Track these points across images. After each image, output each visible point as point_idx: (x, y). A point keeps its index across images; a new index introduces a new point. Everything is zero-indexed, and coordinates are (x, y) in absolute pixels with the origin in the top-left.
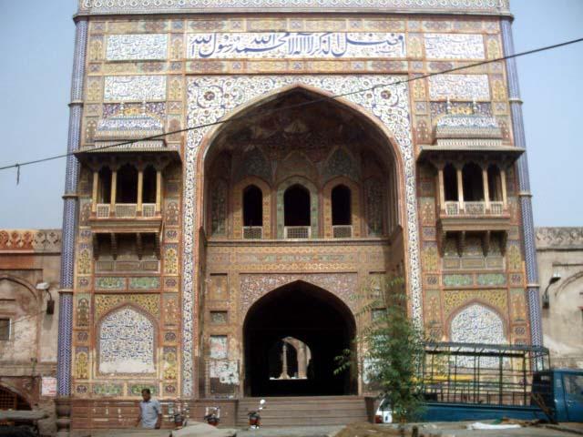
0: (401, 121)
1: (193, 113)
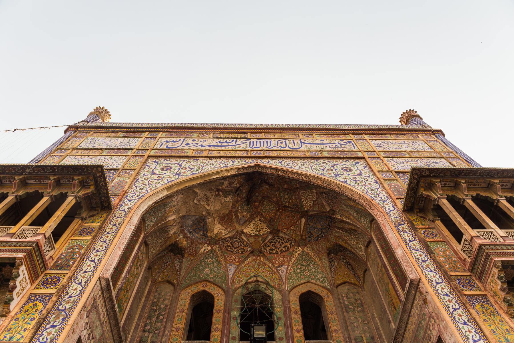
0: (370, 184)
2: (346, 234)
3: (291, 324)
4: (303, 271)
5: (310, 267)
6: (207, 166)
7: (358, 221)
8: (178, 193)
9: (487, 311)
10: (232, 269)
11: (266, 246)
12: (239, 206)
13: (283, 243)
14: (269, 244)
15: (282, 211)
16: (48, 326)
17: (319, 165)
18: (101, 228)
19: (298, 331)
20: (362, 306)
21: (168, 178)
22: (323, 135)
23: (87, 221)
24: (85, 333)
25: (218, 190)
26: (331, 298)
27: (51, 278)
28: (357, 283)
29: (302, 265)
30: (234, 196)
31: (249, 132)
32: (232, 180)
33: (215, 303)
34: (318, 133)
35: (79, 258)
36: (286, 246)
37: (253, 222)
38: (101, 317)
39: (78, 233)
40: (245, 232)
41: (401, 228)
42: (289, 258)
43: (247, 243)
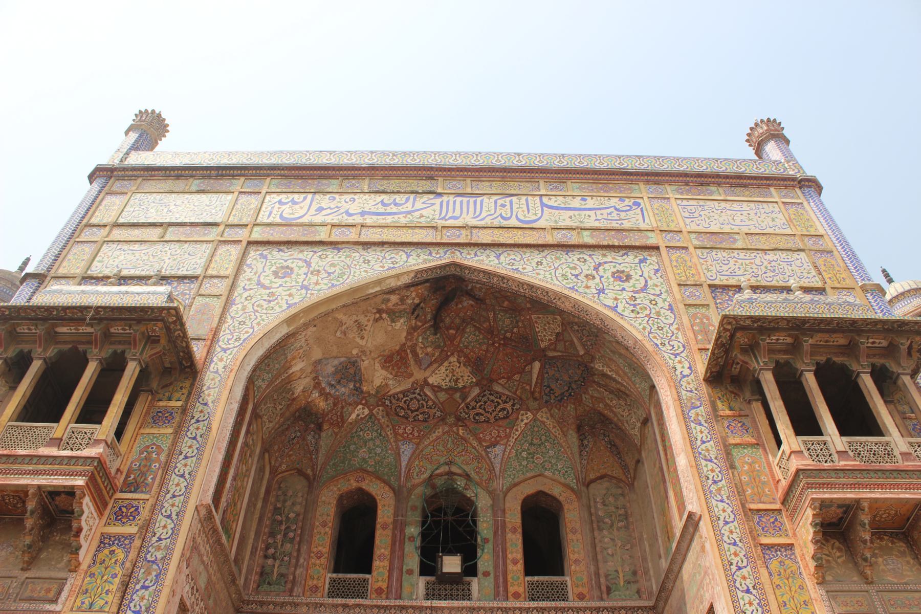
0: (658, 314)
1: (247, 294)
2: (611, 396)
3: (504, 551)
4: (531, 455)
5: (546, 447)
6: (358, 267)
7: (631, 380)
8: (306, 326)
9: (785, 571)
10: (407, 450)
11: (468, 407)
12: (418, 336)
13: (499, 404)
14: (473, 404)
15: (499, 346)
16: (138, 587)
17: (572, 265)
18: (184, 410)
19: (515, 562)
20: (626, 518)
21: (287, 297)
22: (586, 186)
23: (161, 396)
24: (187, 588)
25: (380, 311)
26: (576, 504)
27: (126, 507)
28: (624, 478)
29: (531, 444)
30: (409, 320)
31: (440, 176)
32: (405, 292)
33: (379, 512)
34: (578, 179)
35: (160, 472)
36: (504, 409)
37: (446, 364)
38: (205, 558)
39: (151, 420)
40: (431, 383)
41: (693, 416)
42: (508, 431)
43: (434, 403)
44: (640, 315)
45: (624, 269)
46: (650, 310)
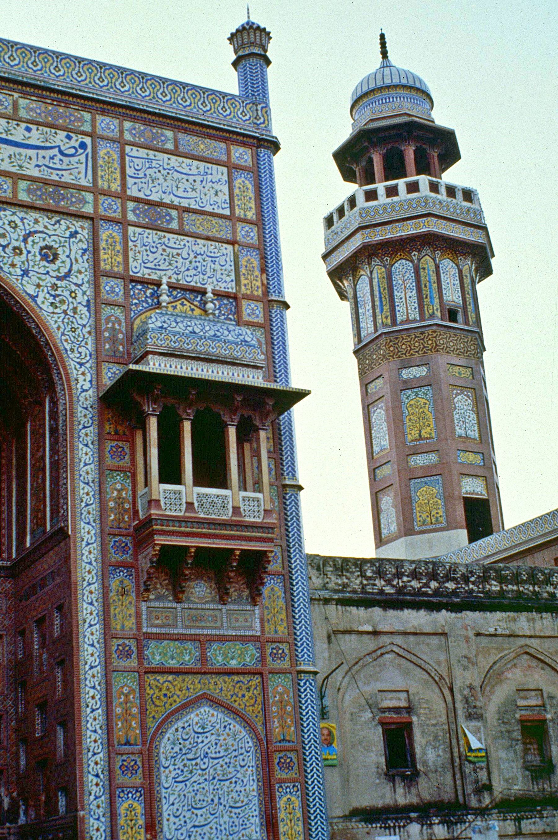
0: (75, 310)
44: (58, 310)
45: (53, 244)
46: (68, 305)
